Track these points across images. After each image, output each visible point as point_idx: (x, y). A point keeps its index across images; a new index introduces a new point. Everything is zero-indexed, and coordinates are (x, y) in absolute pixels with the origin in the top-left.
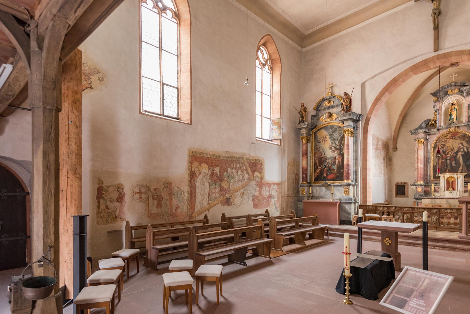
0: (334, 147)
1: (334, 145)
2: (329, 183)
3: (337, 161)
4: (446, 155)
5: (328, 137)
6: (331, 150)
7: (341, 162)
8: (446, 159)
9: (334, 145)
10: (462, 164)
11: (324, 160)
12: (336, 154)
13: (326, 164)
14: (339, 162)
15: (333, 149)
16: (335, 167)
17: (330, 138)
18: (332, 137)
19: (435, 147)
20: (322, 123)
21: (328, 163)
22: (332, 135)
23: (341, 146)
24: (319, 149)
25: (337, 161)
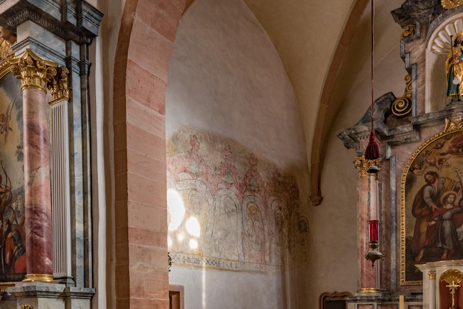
4: (439, 205)
8: (442, 220)
19: (410, 181)
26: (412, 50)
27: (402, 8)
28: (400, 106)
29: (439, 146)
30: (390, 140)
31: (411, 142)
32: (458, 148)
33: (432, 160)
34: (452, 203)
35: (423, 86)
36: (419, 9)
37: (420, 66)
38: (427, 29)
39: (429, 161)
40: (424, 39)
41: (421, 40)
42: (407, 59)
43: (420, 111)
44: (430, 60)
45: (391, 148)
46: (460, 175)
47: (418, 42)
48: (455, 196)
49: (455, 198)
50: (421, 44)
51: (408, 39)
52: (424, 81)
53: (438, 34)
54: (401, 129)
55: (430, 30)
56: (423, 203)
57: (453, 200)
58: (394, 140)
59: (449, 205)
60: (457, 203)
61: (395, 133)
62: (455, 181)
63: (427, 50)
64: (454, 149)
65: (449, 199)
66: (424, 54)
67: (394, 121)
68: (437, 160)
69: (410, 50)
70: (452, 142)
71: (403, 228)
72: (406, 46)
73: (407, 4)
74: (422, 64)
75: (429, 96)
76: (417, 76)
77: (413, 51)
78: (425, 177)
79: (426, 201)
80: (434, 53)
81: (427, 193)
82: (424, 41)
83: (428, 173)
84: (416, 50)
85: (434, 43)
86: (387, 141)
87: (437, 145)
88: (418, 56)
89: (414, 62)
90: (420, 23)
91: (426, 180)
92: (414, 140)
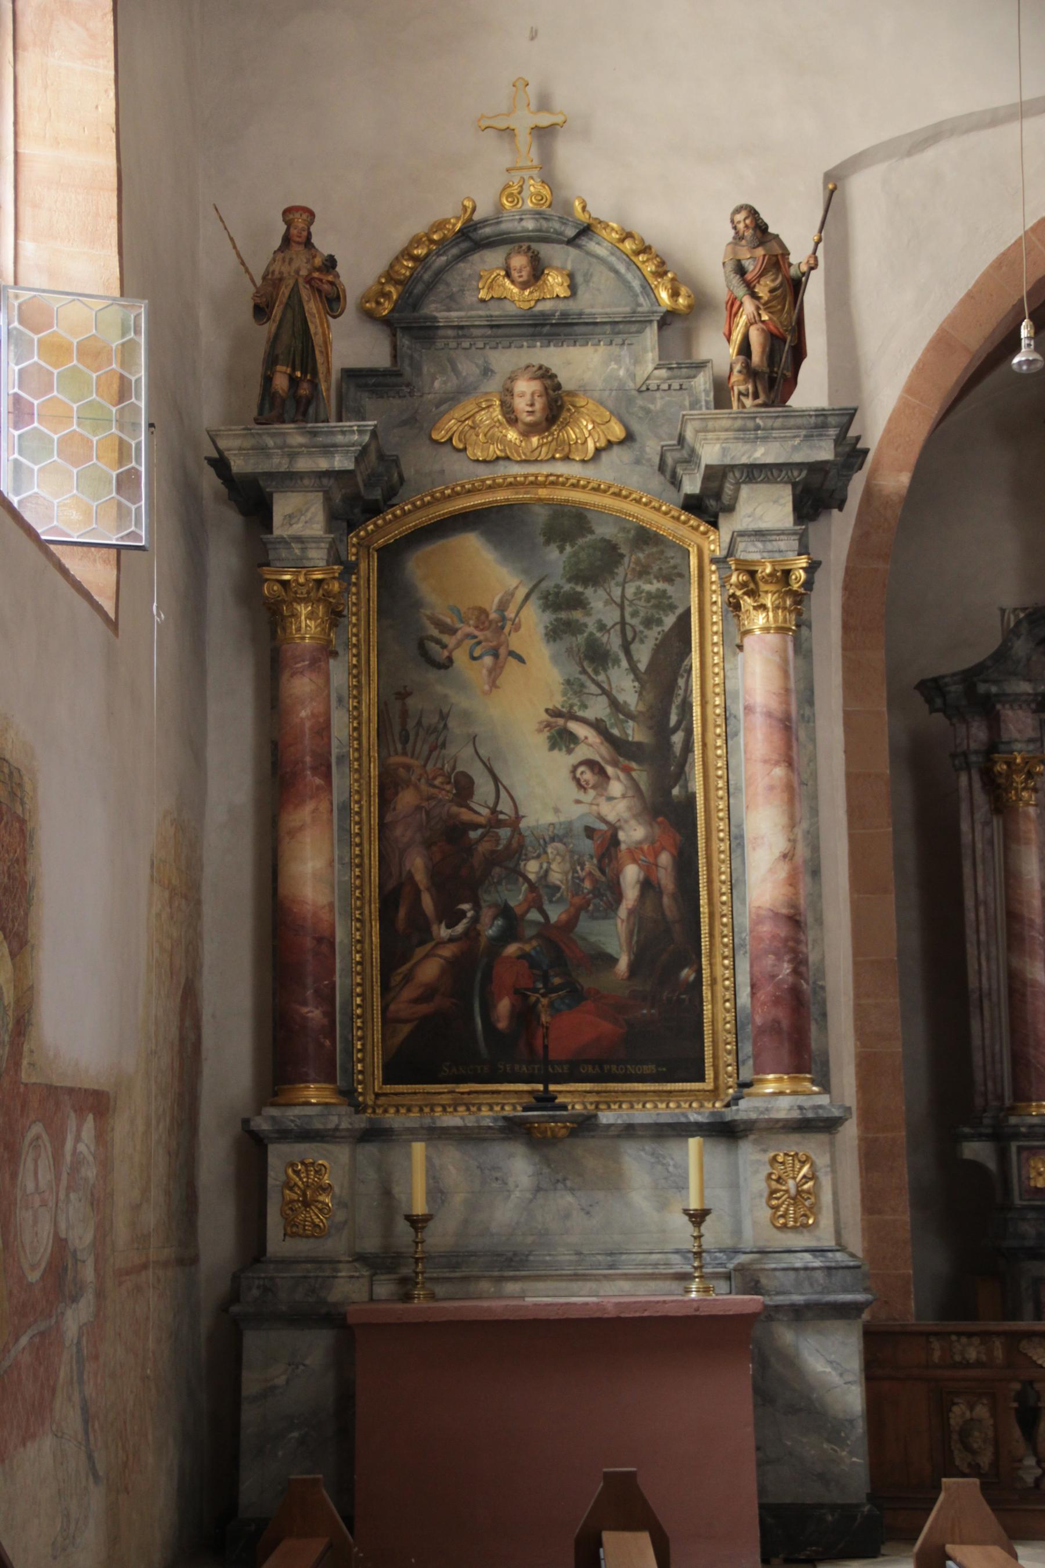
0: (598, 726)
1: (598, 709)
2: (574, 1096)
3: (631, 874)
5: (534, 620)
6: (563, 760)
7: (666, 878)
9: (598, 709)
11: (494, 859)
12: (617, 804)
13: (516, 898)
14: (648, 885)
15: (582, 752)
16: (614, 936)
17: (554, 634)
18: (571, 628)
20: (460, 470)
21: (540, 891)
22: (577, 602)
23: (661, 730)
24: (437, 732)
25: (631, 874)
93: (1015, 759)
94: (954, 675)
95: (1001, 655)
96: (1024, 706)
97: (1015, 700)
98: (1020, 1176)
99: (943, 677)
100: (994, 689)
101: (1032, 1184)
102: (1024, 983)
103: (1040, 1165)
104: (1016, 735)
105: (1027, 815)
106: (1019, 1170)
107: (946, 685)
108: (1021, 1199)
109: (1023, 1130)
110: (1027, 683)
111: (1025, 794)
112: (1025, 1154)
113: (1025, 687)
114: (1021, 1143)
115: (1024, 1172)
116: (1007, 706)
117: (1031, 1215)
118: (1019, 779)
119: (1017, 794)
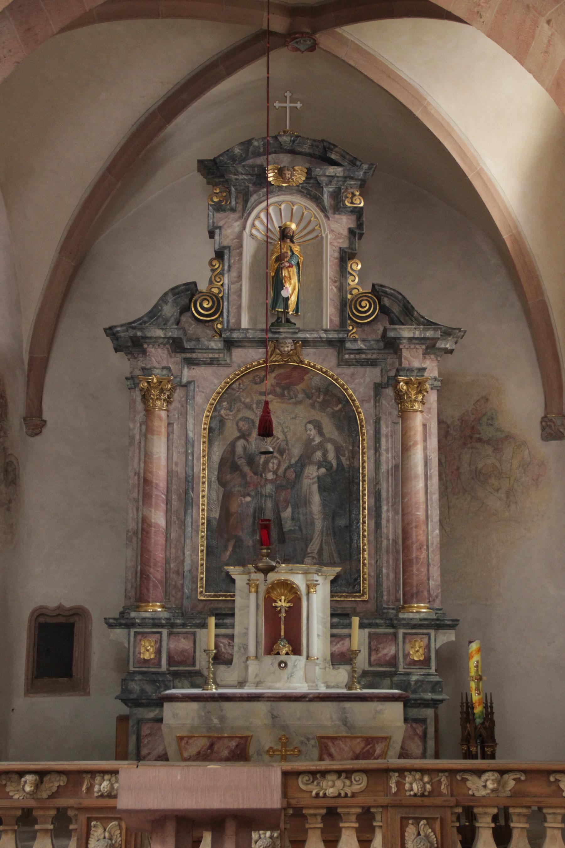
8: (259, 494)
10: (318, 525)
26: (224, 225)
27: (214, 160)
28: (206, 305)
29: (258, 379)
30: (188, 355)
31: (219, 365)
32: (283, 389)
33: (248, 400)
34: (275, 472)
35: (238, 285)
36: (237, 172)
37: (234, 252)
38: (246, 202)
39: (243, 400)
40: (240, 214)
41: (236, 215)
42: (217, 237)
43: (233, 321)
44: (249, 248)
45: (188, 367)
46: (286, 430)
47: (232, 216)
48: (280, 462)
49: (279, 465)
50: (237, 221)
51: (219, 208)
52: (240, 277)
53: (259, 213)
54: (206, 342)
55: (249, 205)
56: (235, 468)
57: (276, 467)
58: (194, 356)
59: (271, 473)
60: (280, 472)
61: (197, 347)
62: (278, 439)
63: (244, 232)
64: (278, 390)
65: (271, 465)
66: (240, 237)
67: (192, 325)
68: (255, 401)
69: (220, 224)
70: (275, 378)
71: (203, 501)
72: (215, 215)
73: (222, 158)
74: (238, 251)
75: (247, 302)
76: (229, 267)
77: (225, 226)
78: (237, 425)
79: (239, 463)
80: (253, 238)
81: (239, 450)
82: (241, 218)
83: (241, 419)
84: (229, 227)
85: (253, 226)
86: (184, 355)
87: (254, 378)
88: (231, 237)
89: (225, 243)
90: (236, 189)
91: (240, 430)
92: (223, 363)
93: (153, 379)
94: (122, 326)
95: (154, 314)
96: (162, 346)
97: (154, 341)
98: (134, 652)
99: (116, 327)
100: (139, 334)
101: (142, 656)
102: (150, 525)
103: (147, 644)
104: (156, 365)
105: (160, 418)
106: (135, 648)
107: (118, 332)
108: (134, 667)
109: (138, 621)
110: (161, 330)
111: (158, 403)
112: (139, 637)
113: (159, 333)
114: (137, 630)
115: (137, 649)
116: (151, 346)
117: (138, 677)
118: (155, 392)
119: (153, 403)
